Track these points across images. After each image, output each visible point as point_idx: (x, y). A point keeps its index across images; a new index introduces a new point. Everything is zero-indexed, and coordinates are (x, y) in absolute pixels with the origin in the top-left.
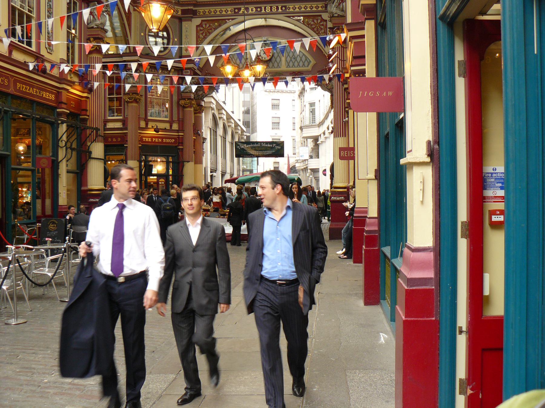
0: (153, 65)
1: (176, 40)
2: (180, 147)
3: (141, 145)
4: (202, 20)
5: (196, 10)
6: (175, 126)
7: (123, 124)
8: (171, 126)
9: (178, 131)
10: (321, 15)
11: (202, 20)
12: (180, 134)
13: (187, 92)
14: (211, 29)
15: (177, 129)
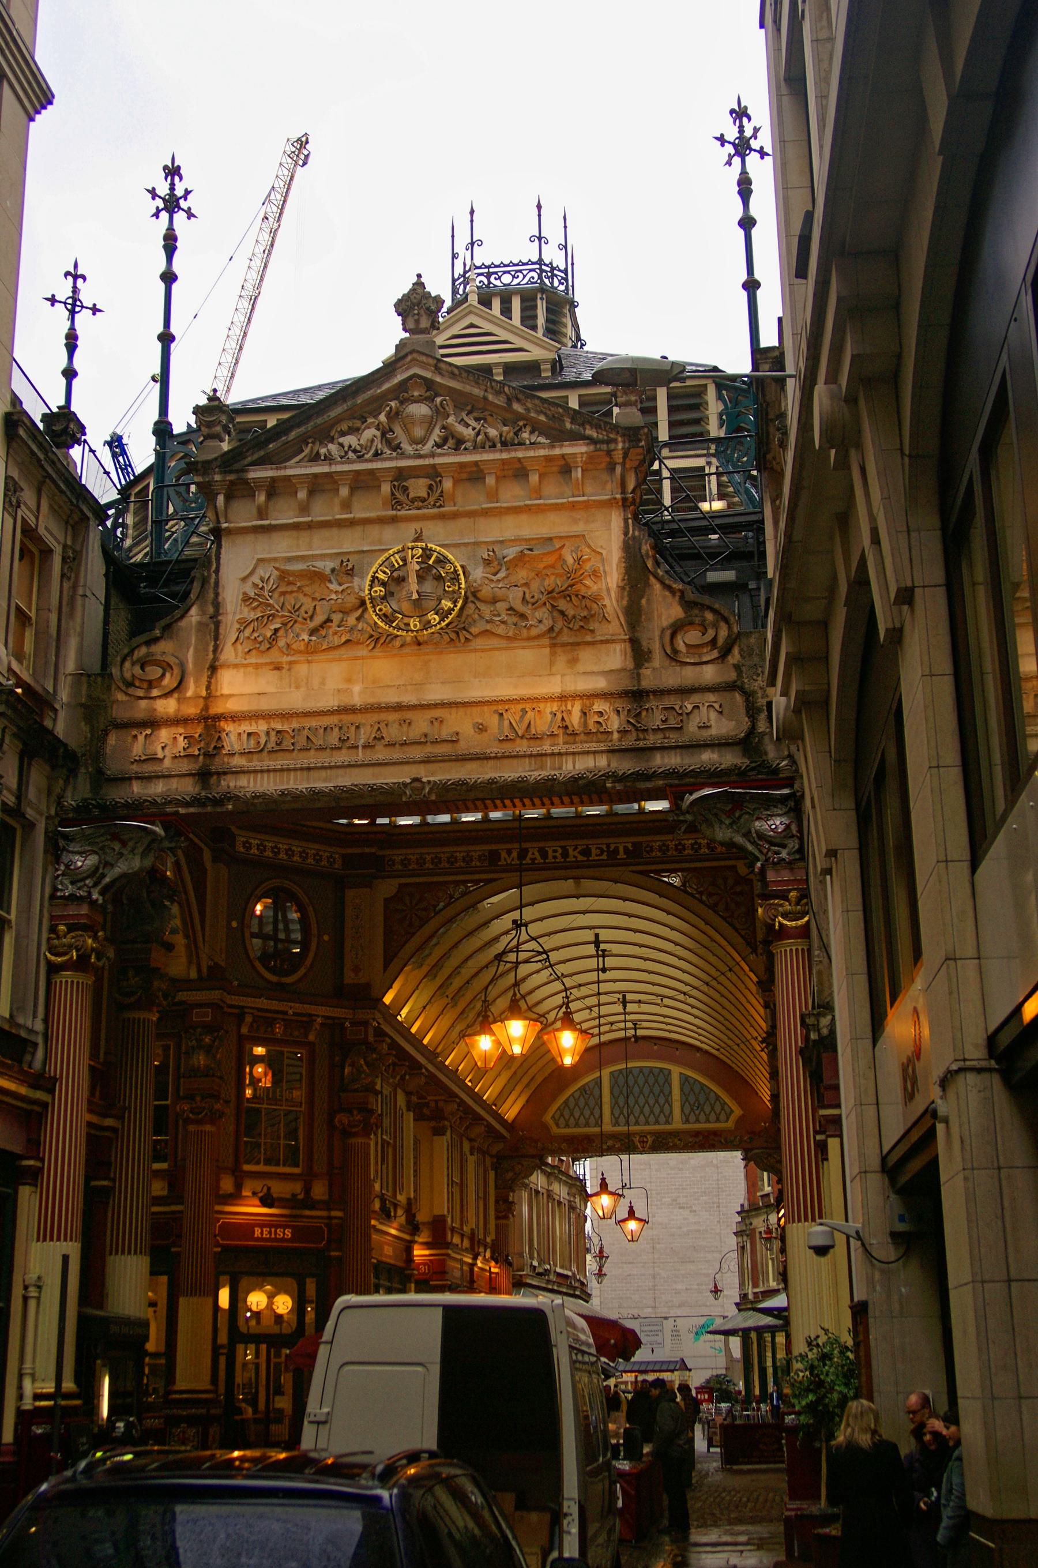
0: (260, 1014)
1: (326, 938)
2: (333, 1254)
3: (219, 1249)
4: (400, 885)
5: (384, 856)
6: (319, 1191)
7: (171, 1186)
8: (307, 1189)
9: (327, 1205)
10: (735, 867)
11: (400, 885)
12: (334, 1213)
13: (356, 1091)
14: (425, 909)
15: (326, 1197)
